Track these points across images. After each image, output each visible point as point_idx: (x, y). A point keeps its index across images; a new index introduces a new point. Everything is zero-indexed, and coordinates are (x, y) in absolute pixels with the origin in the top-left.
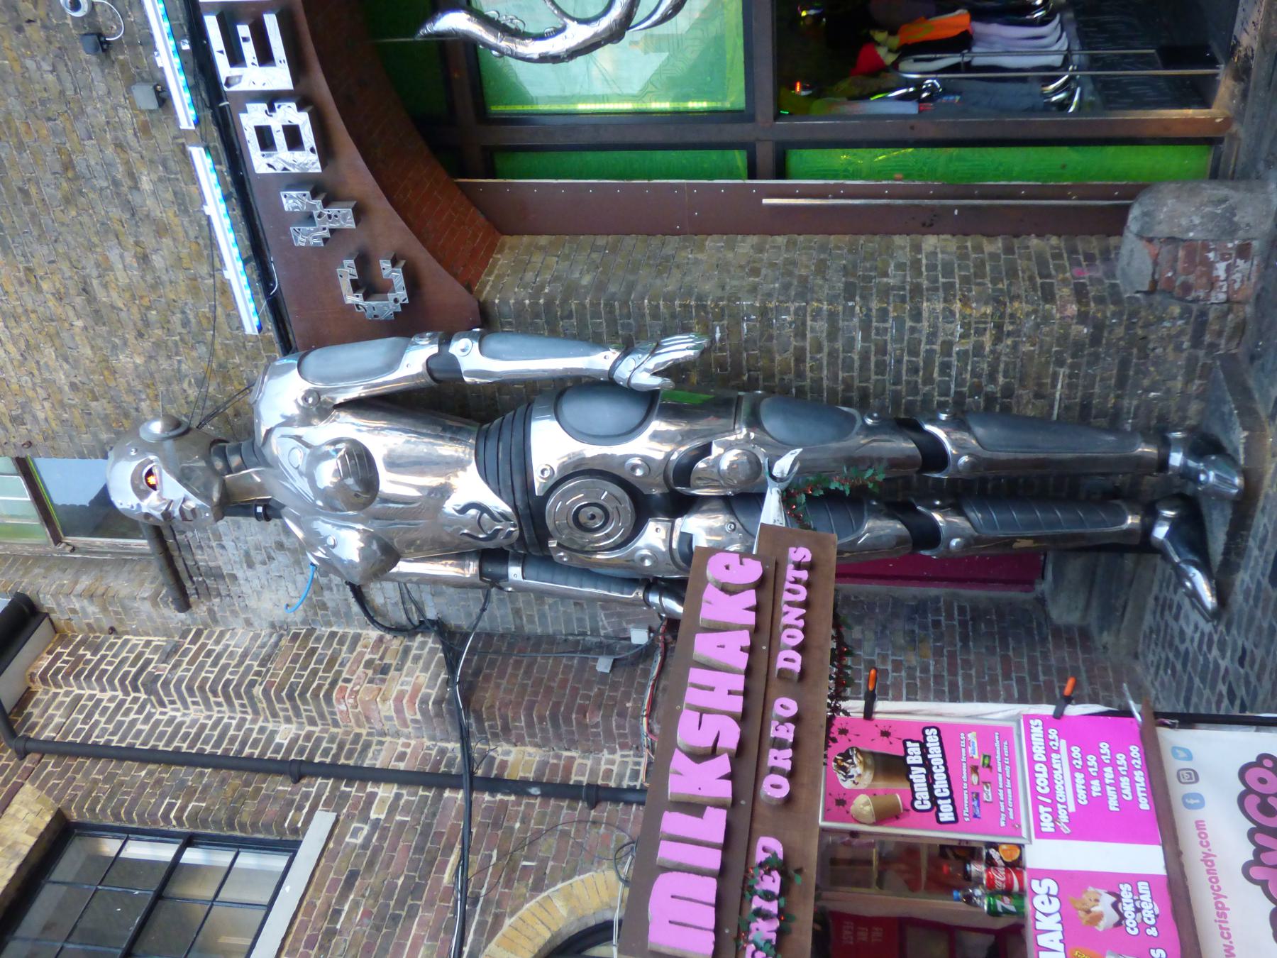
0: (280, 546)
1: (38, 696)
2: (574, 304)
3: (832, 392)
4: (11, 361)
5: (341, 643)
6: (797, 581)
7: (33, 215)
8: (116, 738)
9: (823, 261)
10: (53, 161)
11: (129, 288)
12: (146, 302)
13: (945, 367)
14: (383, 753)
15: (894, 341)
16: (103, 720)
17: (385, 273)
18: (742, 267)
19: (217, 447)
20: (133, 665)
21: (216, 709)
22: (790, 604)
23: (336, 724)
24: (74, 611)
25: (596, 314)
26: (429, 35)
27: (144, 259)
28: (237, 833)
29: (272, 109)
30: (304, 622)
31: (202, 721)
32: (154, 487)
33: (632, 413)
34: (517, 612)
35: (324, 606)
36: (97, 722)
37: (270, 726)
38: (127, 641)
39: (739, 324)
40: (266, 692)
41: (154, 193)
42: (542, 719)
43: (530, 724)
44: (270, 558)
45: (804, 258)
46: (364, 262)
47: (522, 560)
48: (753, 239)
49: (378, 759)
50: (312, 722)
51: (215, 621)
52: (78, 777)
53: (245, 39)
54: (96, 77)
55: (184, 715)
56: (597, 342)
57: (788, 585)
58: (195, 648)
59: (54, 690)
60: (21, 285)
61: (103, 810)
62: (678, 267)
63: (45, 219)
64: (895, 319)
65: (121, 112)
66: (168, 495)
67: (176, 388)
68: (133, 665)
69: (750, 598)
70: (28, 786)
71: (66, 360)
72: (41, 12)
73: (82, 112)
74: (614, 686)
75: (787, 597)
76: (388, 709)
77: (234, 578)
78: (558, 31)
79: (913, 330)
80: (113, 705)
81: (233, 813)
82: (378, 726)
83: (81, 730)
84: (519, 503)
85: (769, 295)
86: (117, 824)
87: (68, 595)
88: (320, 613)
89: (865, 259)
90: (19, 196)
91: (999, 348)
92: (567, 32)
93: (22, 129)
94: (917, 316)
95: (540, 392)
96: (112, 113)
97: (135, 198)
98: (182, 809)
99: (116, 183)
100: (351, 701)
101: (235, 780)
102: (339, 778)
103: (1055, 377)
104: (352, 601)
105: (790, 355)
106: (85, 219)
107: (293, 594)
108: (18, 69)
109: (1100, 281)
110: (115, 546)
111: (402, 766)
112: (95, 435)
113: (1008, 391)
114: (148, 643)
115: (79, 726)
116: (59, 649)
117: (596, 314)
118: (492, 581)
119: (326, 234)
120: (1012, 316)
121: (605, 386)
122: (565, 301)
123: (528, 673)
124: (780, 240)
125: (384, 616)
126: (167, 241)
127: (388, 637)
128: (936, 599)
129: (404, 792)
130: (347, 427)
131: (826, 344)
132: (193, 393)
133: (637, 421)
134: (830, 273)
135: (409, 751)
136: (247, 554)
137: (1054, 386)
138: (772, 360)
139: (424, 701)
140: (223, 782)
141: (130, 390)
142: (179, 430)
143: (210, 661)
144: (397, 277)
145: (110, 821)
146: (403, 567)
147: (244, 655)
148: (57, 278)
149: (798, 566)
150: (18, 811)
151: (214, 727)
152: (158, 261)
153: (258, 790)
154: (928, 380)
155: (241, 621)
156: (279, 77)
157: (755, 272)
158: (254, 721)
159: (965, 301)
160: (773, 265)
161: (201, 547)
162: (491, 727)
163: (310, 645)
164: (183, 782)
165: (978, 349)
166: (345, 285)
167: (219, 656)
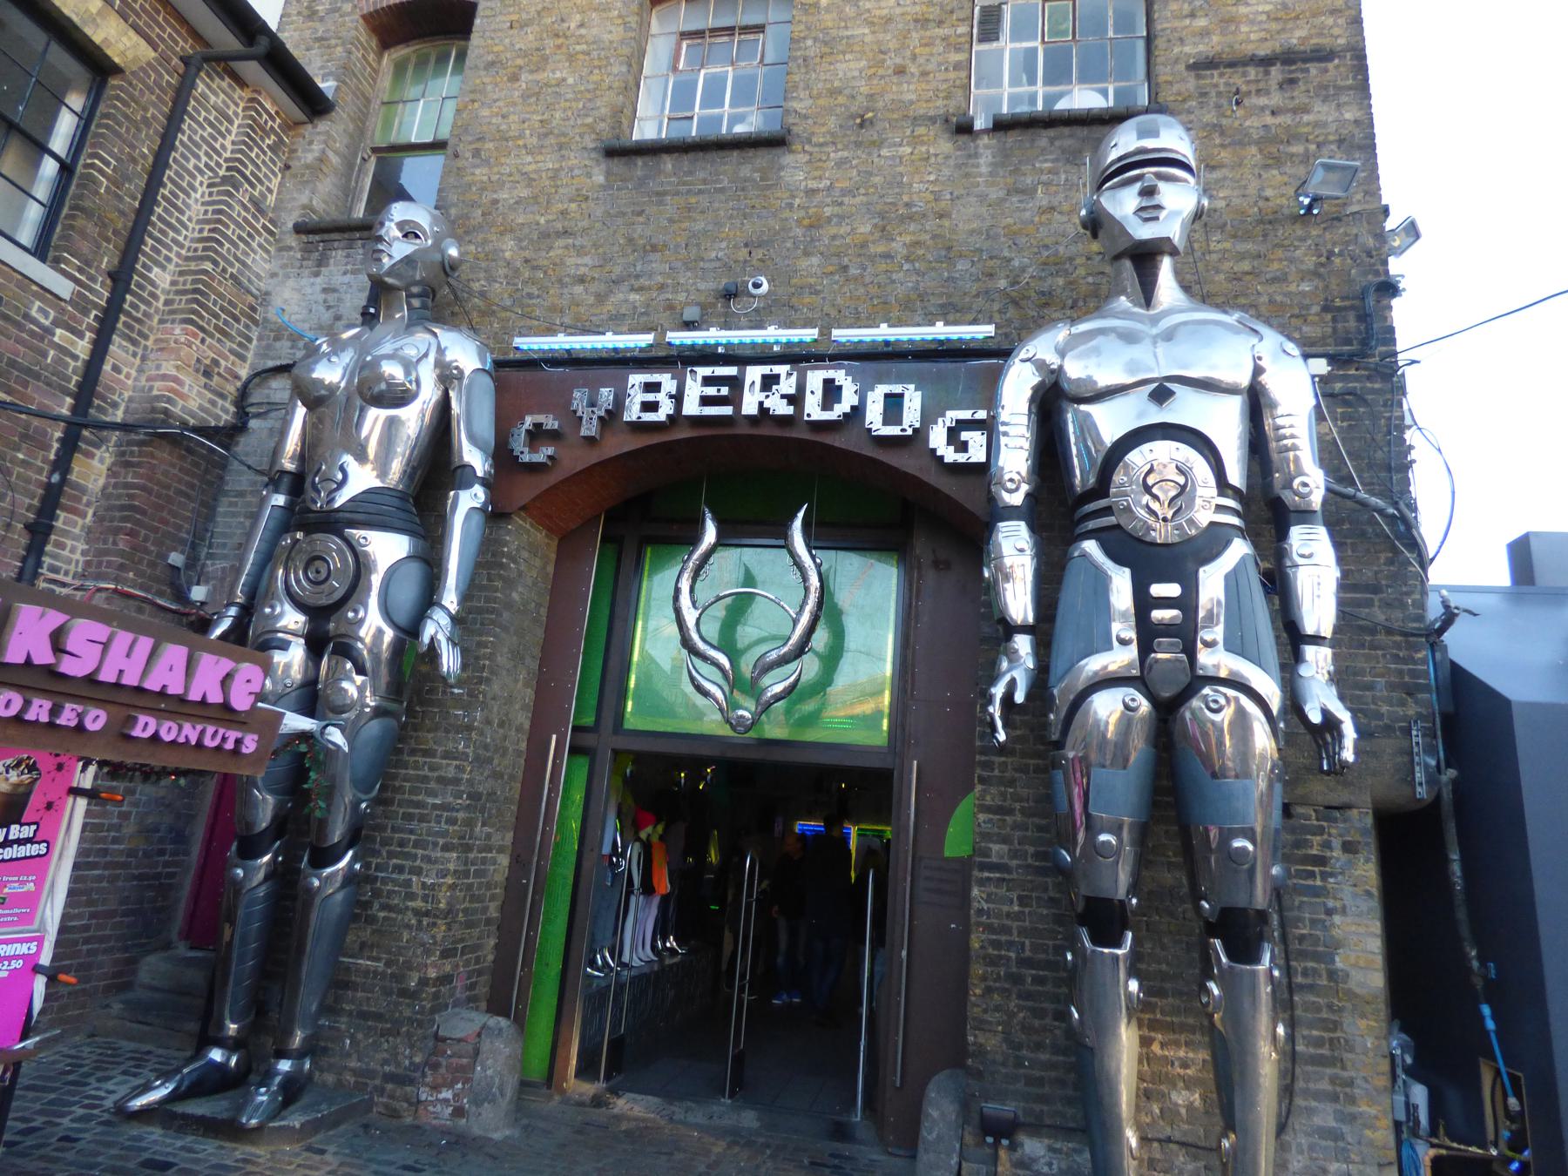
0: (338, 318)
1: (239, 91)
2: (499, 584)
3: (395, 777)
4: (523, 164)
5: (240, 345)
6: (224, 739)
7: (624, 214)
8: (185, 139)
9: (501, 776)
10: (659, 239)
11: (563, 263)
12: (550, 272)
13: (400, 869)
14: (124, 355)
15: (429, 829)
16: (205, 135)
17: (544, 449)
18: (507, 715)
19: (429, 292)
20: (252, 173)
21: (197, 227)
22: (203, 732)
23: (161, 321)
24: (311, 143)
25: (487, 600)
26: (704, 514)
27: (581, 280)
28: (65, 211)
29: (671, 397)
30: (266, 320)
31: (188, 213)
32: (405, 236)
33: (403, 617)
34: (241, 494)
35: (277, 339)
36: (204, 129)
37: (171, 267)
38: (275, 174)
39: (462, 708)
40: (205, 272)
41: (626, 301)
42: (131, 497)
43: (127, 486)
44: (328, 308)
45: (506, 762)
46: (554, 436)
47: (289, 508)
48: (527, 725)
49: (118, 348)
50: (167, 303)
51: (280, 250)
52: (154, 98)
53: (719, 391)
54: (709, 285)
55: (197, 200)
56: (465, 597)
57: (221, 731)
58: (259, 226)
59: (242, 105)
60: (577, 190)
61: (115, 107)
62: (515, 666)
63: (620, 221)
64: (447, 831)
65: (685, 294)
66: (396, 245)
67: (482, 275)
68: (252, 173)
69: (215, 697)
70: (153, 54)
71: (516, 203)
72: (754, 262)
73: (688, 269)
74: (152, 565)
75: (210, 729)
76: (168, 368)
77: (317, 275)
78: (694, 603)
79: (435, 844)
80: (218, 146)
81: (88, 214)
82: (152, 356)
83: (199, 114)
84: (341, 514)
85: (482, 733)
86: (98, 114)
87: (325, 142)
88: (272, 334)
89: (499, 810)
90: (638, 209)
91: (409, 913)
92: (692, 610)
93: (684, 225)
94: (446, 848)
95: (432, 548)
97: (625, 286)
98: (101, 171)
99: (637, 277)
100: (183, 340)
101: (123, 224)
102: (106, 311)
103: (377, 959)
104: (278, 363)
105: (431, 745)
106: (616, 248)
107: (293, 317)
108: (724, 235)
109: (452, 995)
110: (361, 191)
111: (107, 367)
112: (455, 205)
113: (371, 920)
114: (270, 190)
115: (203, 113)
116: (278, 121)
117: (487, 600)
118: (275, 480)
119: (579, 413)
120: (434, 924)
121: (429, 597)
122: (501, 577)
123: (180, 493)
124: (523, 746)
125: (258, 385)
126: (592, 300)
127: (239, 384)
128: (187, 853)
129: (79, 364)
130: (429, 393)
131: (436, 774)
132: (476, 286)
133: (395, 619)
134: (491, 782)
135: (122, 377)
136: (335, 290)
137: (369, 959)
138: (428, 731)
139: (169, 401)
140: (122, 213)
141: (485, 242)
142: (448, 268)
143: (245, 235)
144: (540, 457)
145: (102, 108)
146: (301, 411)
147: (244, 264)
148: (578, 216)
149: (238, 742)
150: (130, 39)
151: (178, 220)
152: (579, 289)
153: (108, 240)
154: (391, 855)
155: (276, 270)
156: (691, 407)
157: (501, 724)
158: (178, 255)
159: (452, 887)
160: (505, 738)
161: (348, 256)
162: (132, 453)
163: (243, 319)
164: (130, 181)
165: (411, 896)
166: (540, 418)
167: (247, 244)
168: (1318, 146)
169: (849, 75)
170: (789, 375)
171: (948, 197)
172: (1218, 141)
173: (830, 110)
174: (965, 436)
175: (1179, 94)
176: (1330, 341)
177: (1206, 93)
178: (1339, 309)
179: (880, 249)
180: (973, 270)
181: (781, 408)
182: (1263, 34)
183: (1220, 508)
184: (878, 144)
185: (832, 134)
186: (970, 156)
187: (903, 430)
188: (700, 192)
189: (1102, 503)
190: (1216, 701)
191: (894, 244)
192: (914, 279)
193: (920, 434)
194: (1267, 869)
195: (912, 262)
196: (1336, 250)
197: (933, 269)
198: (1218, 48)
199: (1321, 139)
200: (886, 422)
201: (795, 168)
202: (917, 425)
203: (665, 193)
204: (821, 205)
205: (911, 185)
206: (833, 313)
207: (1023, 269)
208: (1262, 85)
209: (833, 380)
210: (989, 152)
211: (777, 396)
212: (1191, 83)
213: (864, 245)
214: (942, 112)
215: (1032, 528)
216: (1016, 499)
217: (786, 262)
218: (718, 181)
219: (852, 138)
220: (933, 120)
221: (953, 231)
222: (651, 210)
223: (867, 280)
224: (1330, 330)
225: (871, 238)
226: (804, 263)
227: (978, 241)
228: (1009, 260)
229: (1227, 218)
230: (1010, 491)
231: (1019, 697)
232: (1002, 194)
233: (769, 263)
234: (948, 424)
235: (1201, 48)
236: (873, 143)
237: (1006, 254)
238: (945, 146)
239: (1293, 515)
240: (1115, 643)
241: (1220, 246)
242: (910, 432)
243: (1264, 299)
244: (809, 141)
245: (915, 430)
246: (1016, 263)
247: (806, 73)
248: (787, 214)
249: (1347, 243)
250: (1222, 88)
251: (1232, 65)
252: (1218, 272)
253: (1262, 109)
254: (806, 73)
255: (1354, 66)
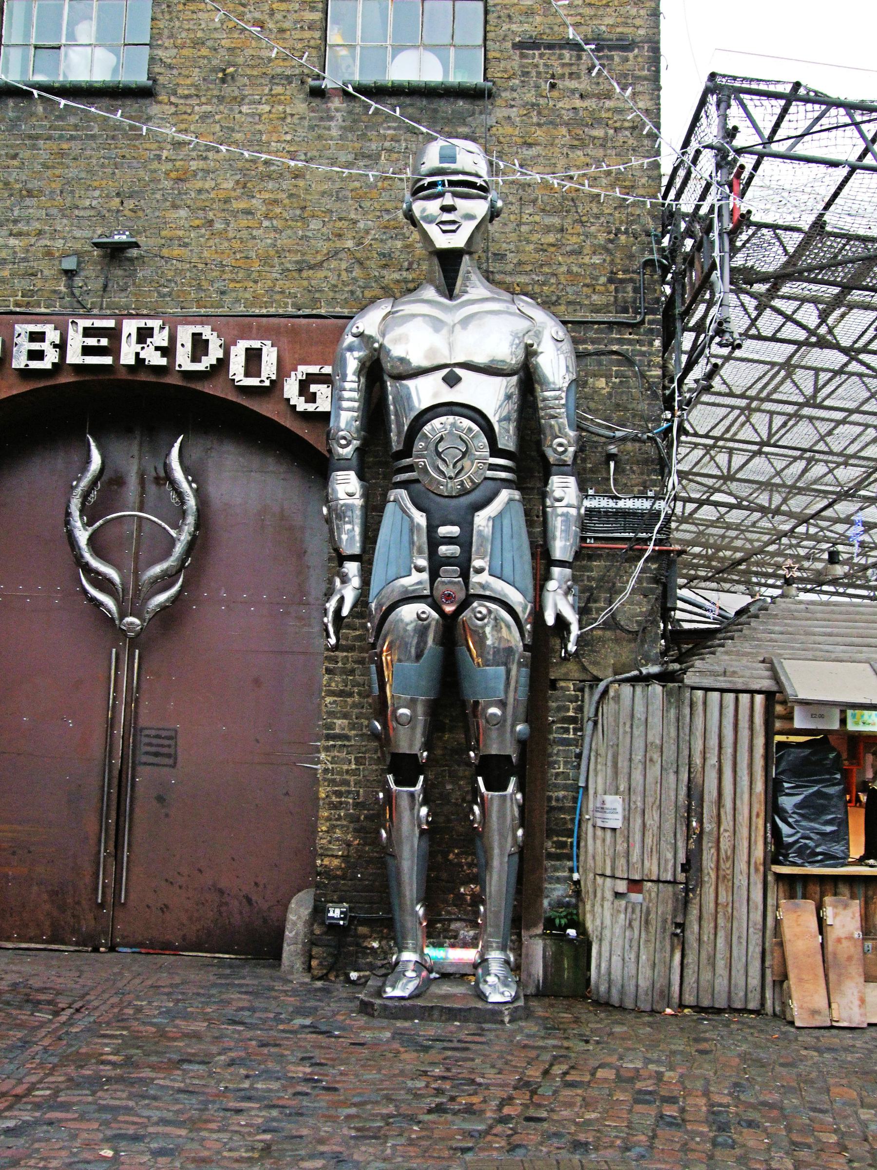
10: (34, 185)
73: (64, 216)
90: (12, 152)
93: (57, 172)
96: (62, 235)
99: (15, 222)
108: (95, 184)
156: (74, 357)
168: (616, 130)
169: (212, 26)
170: (162, 328)
171: (303, 157)
172: (535, 120)
173: (194, 62)
174: (313, 388)
175: (505, 71)
176: (612, 308)
177: (528, 73)
178: (622, 281)
179: (242, 205)
180: (324, 230)
181: (156, 359)
182: (578, 19)
183: (492, 467)
184: (240, 100)
185: (197, 87)
186: (321, 119)
187: (262, 381)
188: (72, 138)
189: (407, 461)
190: (480, 612)
191: (254, 201)
192: (272, 235)
193: (276, 385)
194: (513, 726)
195: (271, 219)
196: (623, 228)
197: (290, 227)
198: (540, 29)
199: (618, 125)
200: (247, 374)
201: (162, 119)
202: (274, 377)
203: (37, 137)
204: (189, 159)
205: (269, 143)
206: (200, 266)
207: (367, 232)
208: (574, 69)
209: (201, 334)
210: (339, 115)
211: (152, 348)
212: (515, 62)
213: (227, 201)
214: (297, 72)
215: (361, 477)
216: (347, 452)
217: (157, 214)
218: (90, 128)
219: (216, 93)
220: (289, 79)
221: (307, 190)
222: (25, 154)
223: (231, 235)
224: (612, 299)
225: (233, 194)
226: (172, 215)
227: (328, 203)
228: (355, 222)
229: (539, 193)
230: (343, 447)
231: (345, 612)
232: (350, 158)
233: (140, 214)
234: (300, 377)
235: (526, 27)
236: (235, 98)
237: (353, 216)
238: (301, 107)
239: (554, 469)
240: (413, 571)
241: (531, 219)
242: (267, 383)
243: (564, 269)
244: (175, 94)
245: (272, 382)
246: (361, 225)
247: (171, 20)
248: (155, 165)
249: (632, 223)
250: (541, 69)
251: (550, 46)
252: (528, 242)
253: (573, 91)
254: (171, 20)
255: (649, 58)
